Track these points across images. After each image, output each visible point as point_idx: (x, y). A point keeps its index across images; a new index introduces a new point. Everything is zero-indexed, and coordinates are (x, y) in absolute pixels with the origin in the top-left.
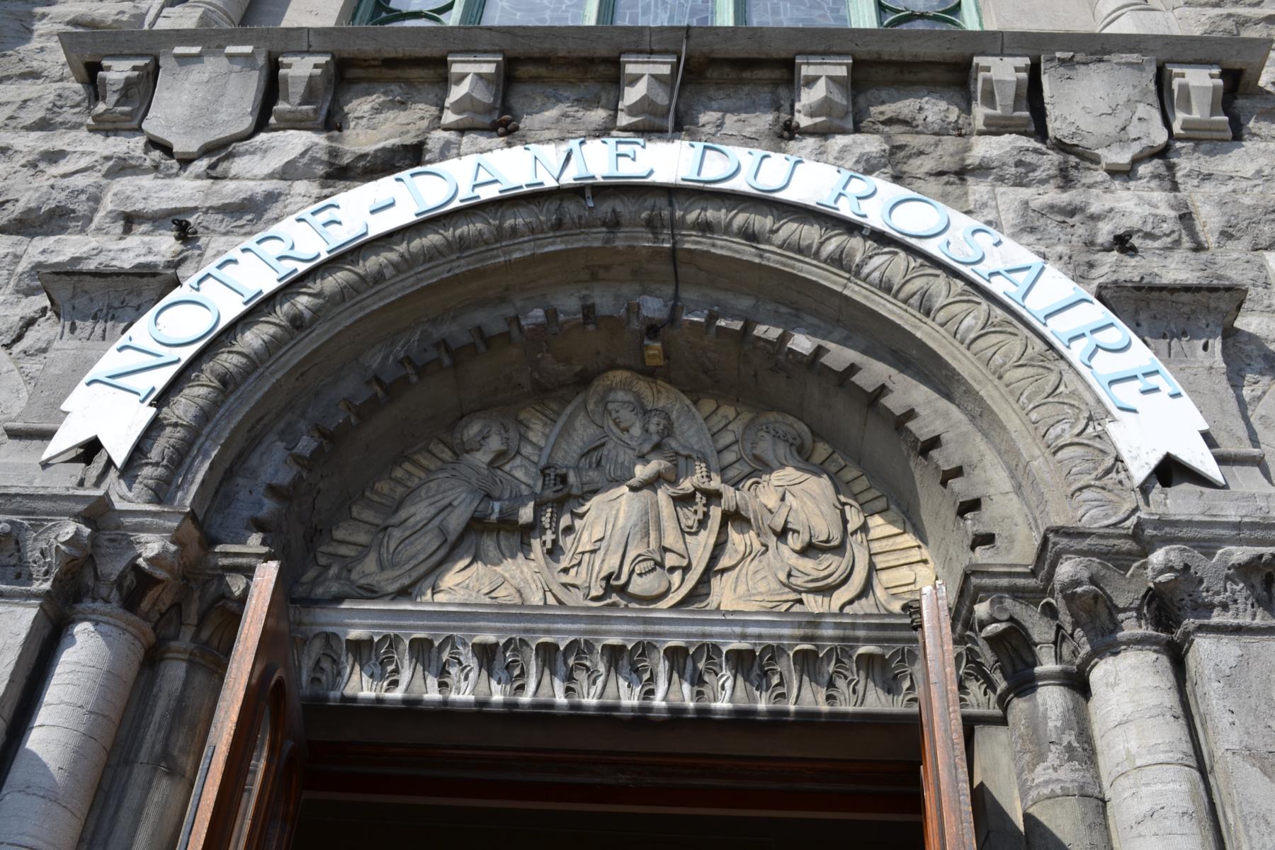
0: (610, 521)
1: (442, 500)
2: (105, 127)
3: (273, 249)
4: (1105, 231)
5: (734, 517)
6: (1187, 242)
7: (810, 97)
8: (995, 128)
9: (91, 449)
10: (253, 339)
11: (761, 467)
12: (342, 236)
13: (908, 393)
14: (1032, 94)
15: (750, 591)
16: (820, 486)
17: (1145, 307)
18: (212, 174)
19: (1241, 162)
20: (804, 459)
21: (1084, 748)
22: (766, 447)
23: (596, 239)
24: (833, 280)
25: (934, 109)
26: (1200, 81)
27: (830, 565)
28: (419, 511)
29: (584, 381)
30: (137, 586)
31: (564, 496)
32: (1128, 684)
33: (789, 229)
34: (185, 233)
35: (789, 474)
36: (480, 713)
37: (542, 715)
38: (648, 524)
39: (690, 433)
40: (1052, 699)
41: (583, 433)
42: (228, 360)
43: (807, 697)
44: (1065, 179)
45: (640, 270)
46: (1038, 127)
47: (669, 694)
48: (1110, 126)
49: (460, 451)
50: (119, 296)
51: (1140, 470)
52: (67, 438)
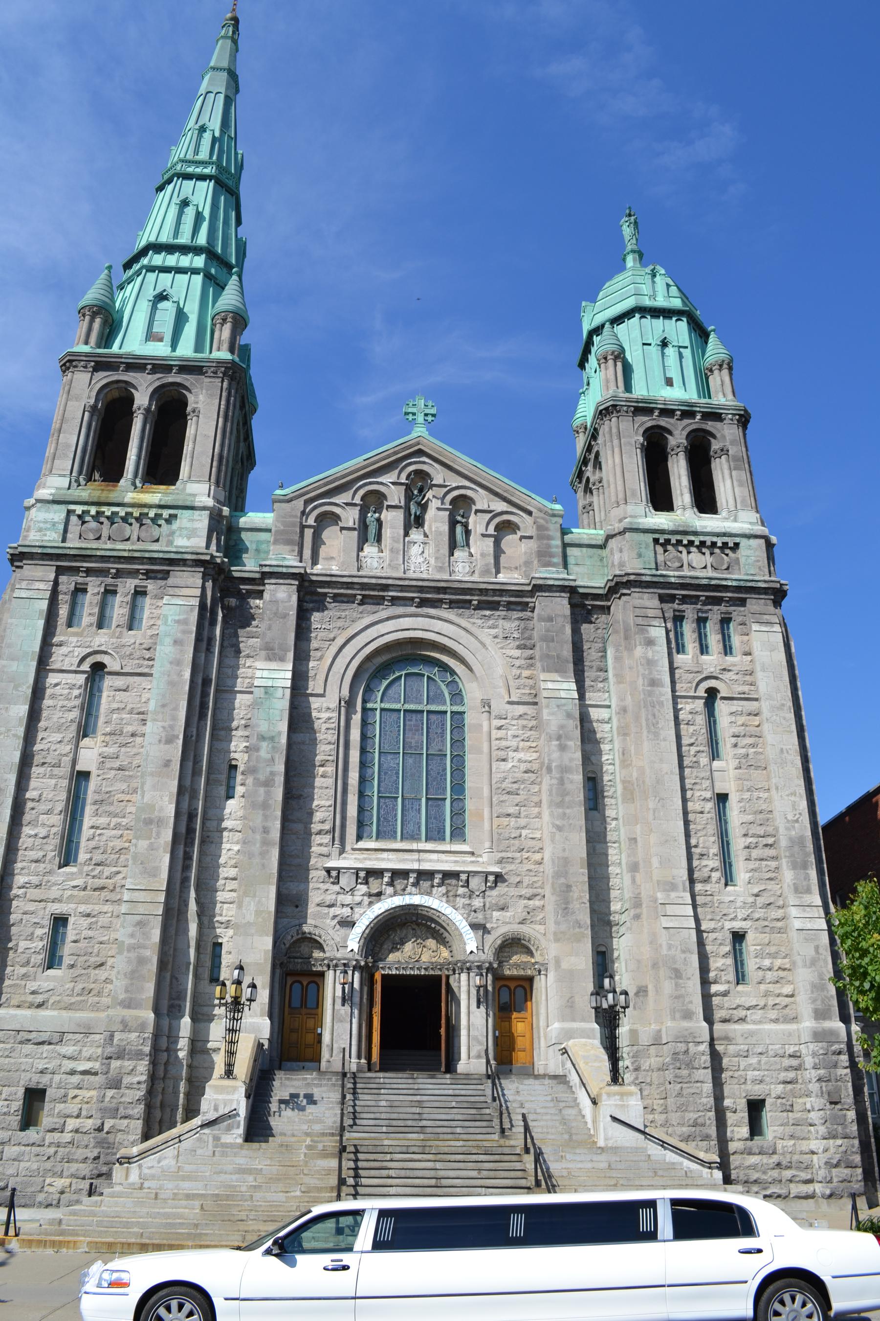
0: (409, 947)
1: (387, 945)
2: (333, 883)
3: (367, 917)
4: (473, 908)
5: (424, 946)
7: (436, 881)
8: (462, 886)
9: (352, 950)
10: (367, 931)
11: (428, 938)
12: (376, 914)
13: (446, 934)
14: (467, 881)
15: (425, 958)
16: (434, 941)
17: (474, 926)
18: (353, 895)
19: (494, 893)
20: (434, 938)
21: (459, 982)
22: (429, 936)
23: (407, 911)
24: (437, 919)
25: (454, 882)
26: (491, 878)
27: (435, 953)
28: (385, 946)
29: (405, 924)
30: (361, 967)
31: (403, 944)
32: (464, 976)
33: (432, 911)
34: (352, 908)
35: (430, 940)
36: (396, 975)
37: (403, 975)
38: (414, 948)
39: (419, 932)
40: (457, 975)
41: (405, 932)
42: (365, 935)
43: (432, 973)
44: (470, 897)
45: (413, 914)
46: (468, 887)
47: (416, 972)
48: (477, 888)
49: (389, 936)
50: (348, 923)
51: (468, 952)
52: (349, 949)
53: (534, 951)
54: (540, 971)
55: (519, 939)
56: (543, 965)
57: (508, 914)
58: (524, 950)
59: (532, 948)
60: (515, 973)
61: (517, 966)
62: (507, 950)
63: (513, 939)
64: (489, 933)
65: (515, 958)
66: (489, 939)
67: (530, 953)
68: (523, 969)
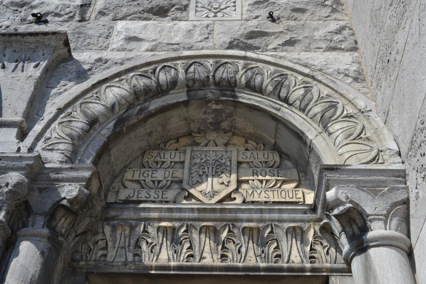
6: (77, 18)
53: (312, 133)
54: (356, 224)
55: (229, 86)
56: (375, 180)
57: (183, 25)
58: (261, 156)
59: (297, 119)
60: (210, 259)
61: (219, 222)
62: (169, 157)
63: (193, 86)
64: (81, 75)
65: (210, 190)
66: (66, 91)
67: (291, 155)
68: (256, 235)
